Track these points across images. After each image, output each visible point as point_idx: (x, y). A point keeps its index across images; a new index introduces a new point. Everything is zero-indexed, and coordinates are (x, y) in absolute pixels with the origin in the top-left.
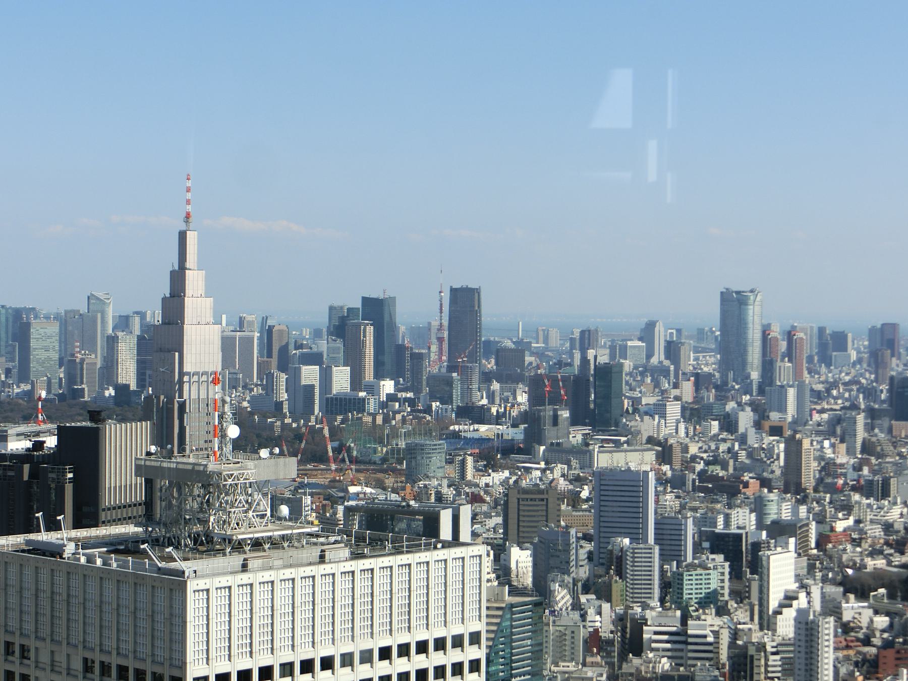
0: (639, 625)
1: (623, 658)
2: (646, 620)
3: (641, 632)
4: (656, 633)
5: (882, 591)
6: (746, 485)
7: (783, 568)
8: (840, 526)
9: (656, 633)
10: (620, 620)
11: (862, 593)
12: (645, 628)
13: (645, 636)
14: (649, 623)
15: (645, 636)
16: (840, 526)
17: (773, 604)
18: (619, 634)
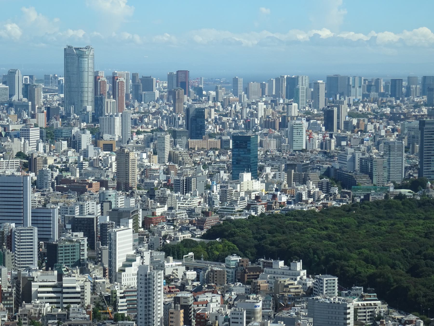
0: (29, 281)
1: (18, 304)
2: (33, 278)
3: (30, 287)
4: (40, 287)
5: (191, 254)
6: (91, 185)
7: (124, 240)
8: (159, 212)
9: (40, 287)
10: (16, 279)
11: (178, 257)
12: (33, 283)
13: (33, 289)
14: (35, 280)
15: (34, 289)
16: (159, 212)
17: (119, 265)
18: (15, 288)
